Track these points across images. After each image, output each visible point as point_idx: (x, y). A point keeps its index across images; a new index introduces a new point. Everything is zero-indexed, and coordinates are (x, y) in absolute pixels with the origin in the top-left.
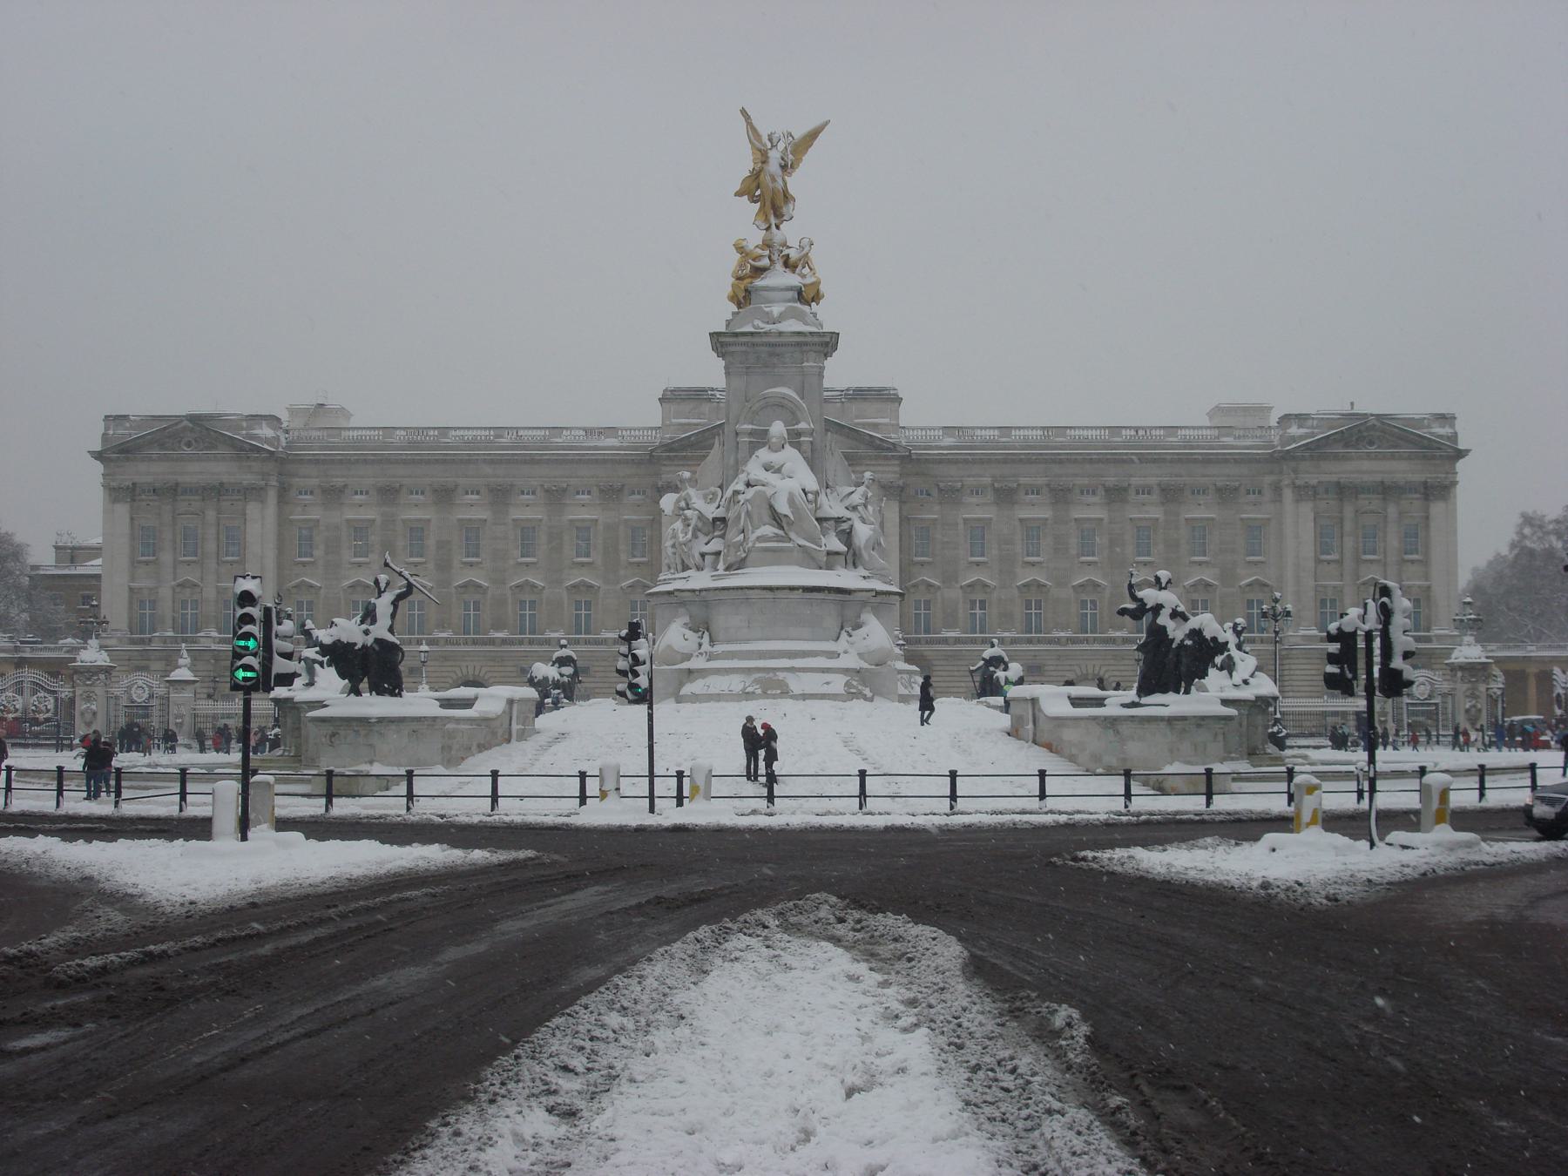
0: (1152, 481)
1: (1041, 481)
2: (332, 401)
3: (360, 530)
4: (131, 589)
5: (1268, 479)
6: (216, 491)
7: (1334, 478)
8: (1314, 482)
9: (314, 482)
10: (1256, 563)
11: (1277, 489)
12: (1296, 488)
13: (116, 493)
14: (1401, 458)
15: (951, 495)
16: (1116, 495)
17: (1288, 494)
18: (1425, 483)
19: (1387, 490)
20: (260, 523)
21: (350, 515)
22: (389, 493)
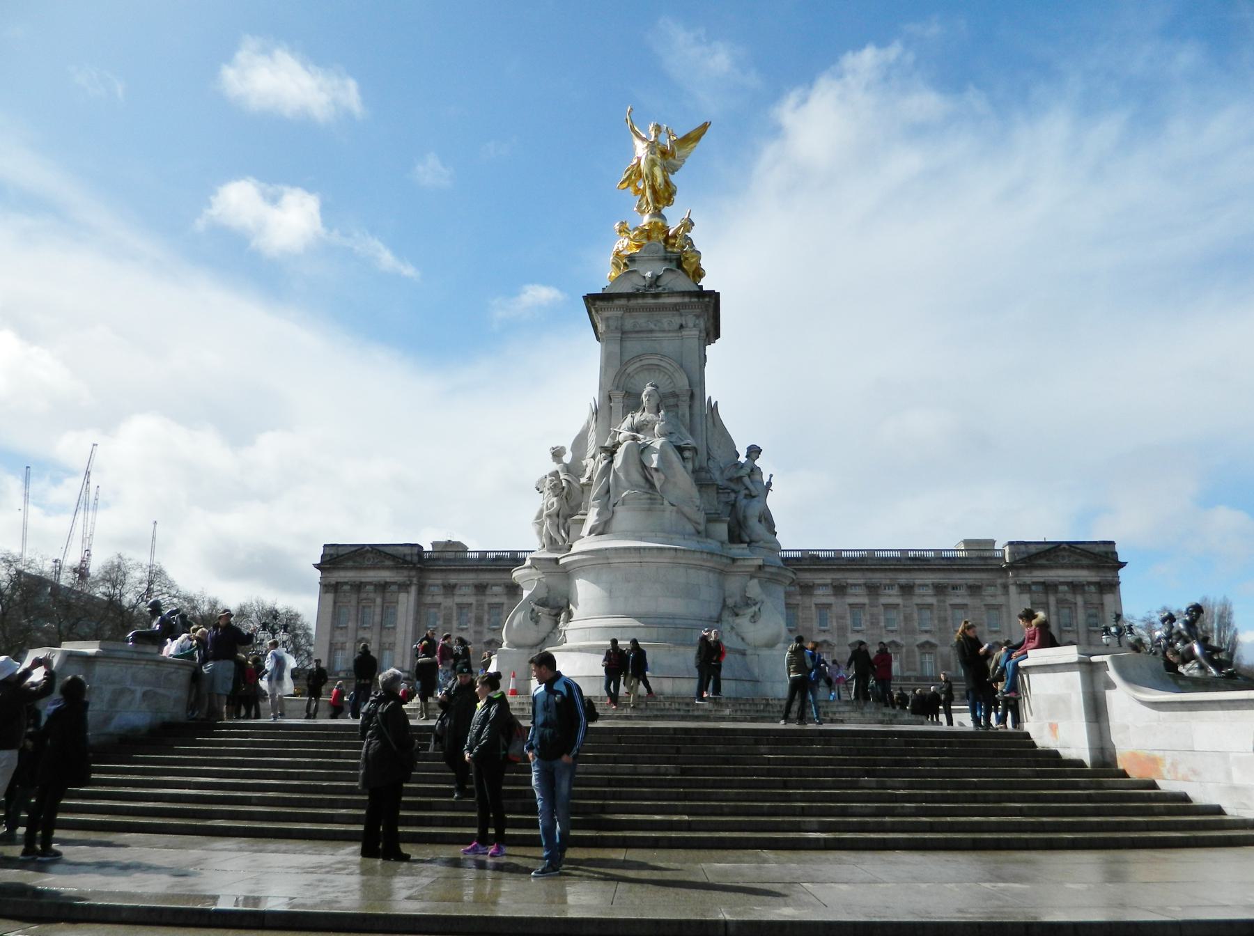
0: (929, 582)
1: (862, 581)
2: (454, 539)
3: (460, 607)
4: (331, 644)
5: (999, 581)
6: (382, 587)
7: (1042, 580)
8: (1029, 582)
9: (439, 582)
10: (996, 632)
11: (1005, 587)
12: (1019, 586)
13: (326, 587)
14: (1082, 567)
15: (807, 589)
16: (907, 589)
17: (1013, 589)
18: (1098, 584)
19: (1075, 587)
20: (406, 603)
21: (458, 600)
22: (481, 588)
